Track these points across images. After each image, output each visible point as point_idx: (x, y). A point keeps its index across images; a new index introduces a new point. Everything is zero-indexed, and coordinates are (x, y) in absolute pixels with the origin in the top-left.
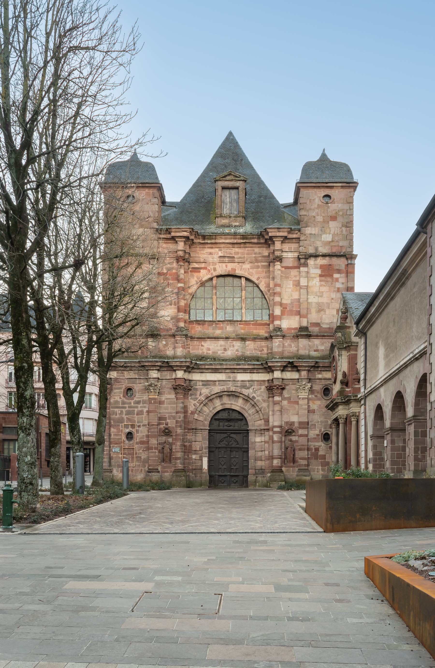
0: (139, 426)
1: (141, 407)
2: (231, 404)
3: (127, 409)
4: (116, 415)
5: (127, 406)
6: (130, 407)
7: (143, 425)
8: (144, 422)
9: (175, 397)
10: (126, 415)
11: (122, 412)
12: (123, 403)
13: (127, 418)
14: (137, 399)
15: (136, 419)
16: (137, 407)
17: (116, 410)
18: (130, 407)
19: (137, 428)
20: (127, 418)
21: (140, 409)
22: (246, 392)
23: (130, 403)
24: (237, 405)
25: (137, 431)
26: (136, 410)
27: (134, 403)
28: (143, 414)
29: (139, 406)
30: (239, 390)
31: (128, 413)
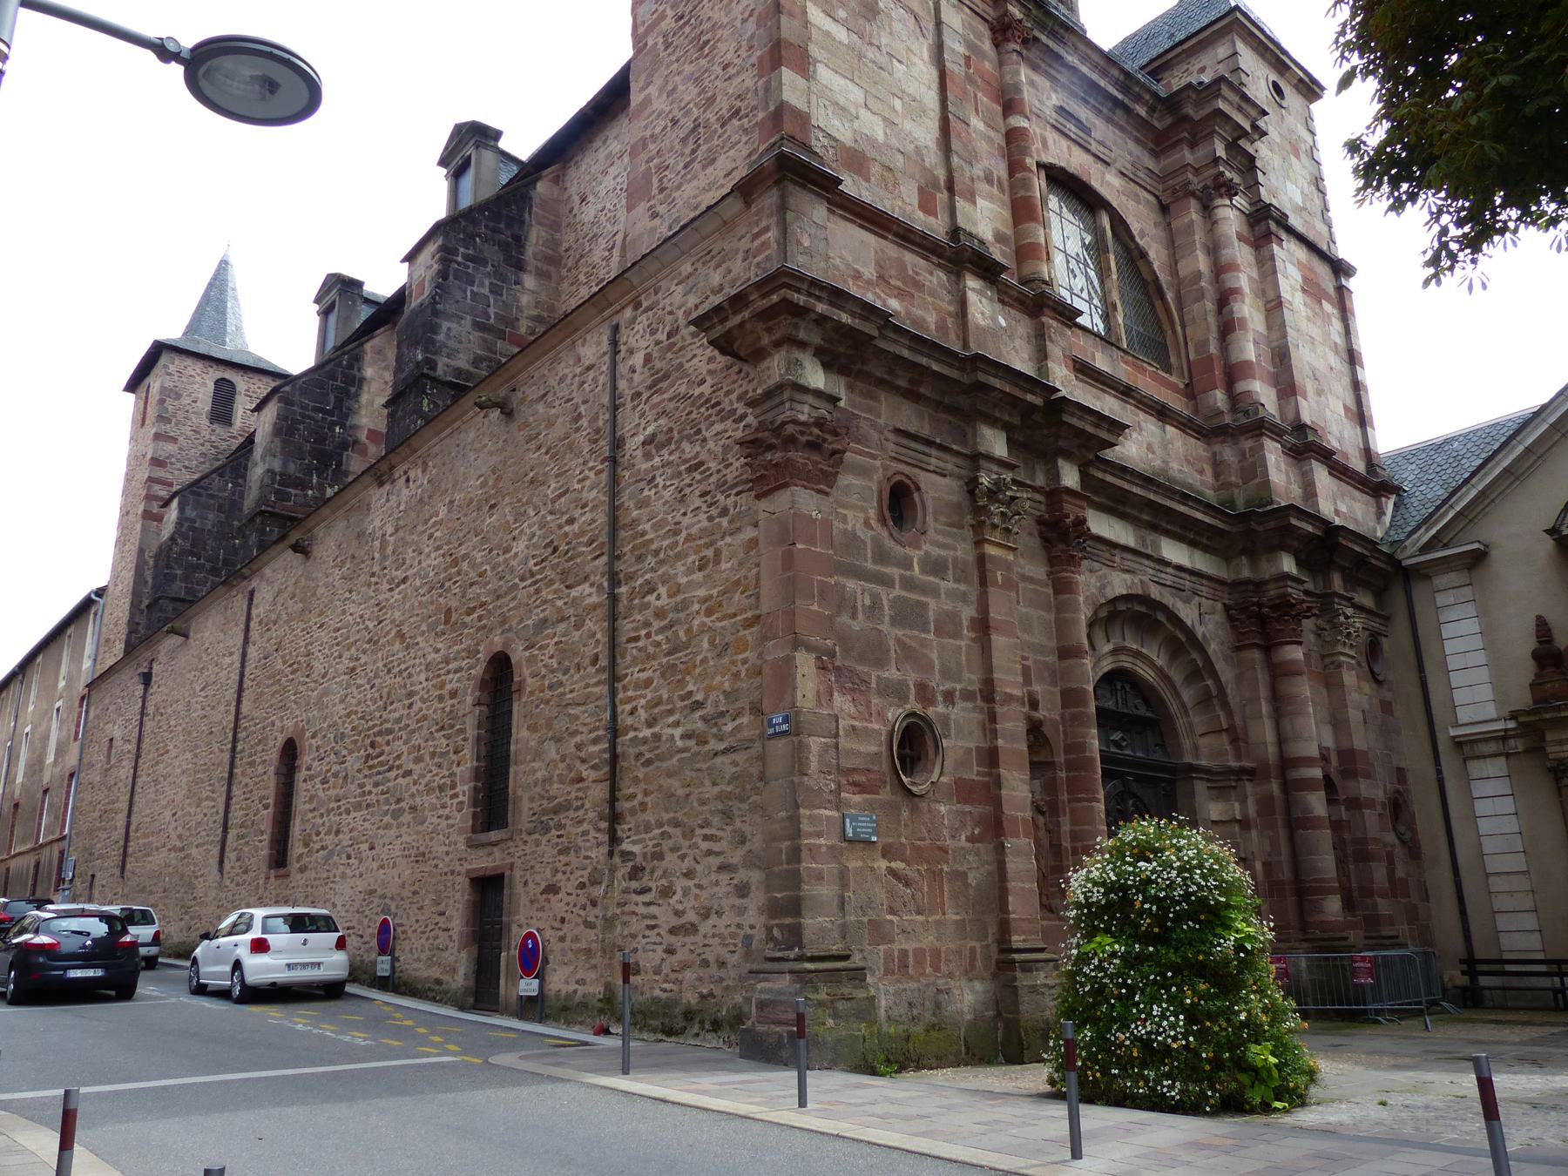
0: (949, 697)
1: (949, 593)
2: (1137, 655)
3: (897, 591)
4: (854, 616)
5: (894, 572)
6: (909, 584)
7: (967, 696)
8: (966, 675)
9: (1049, 574)
10: (895, 622)
11: (875, 607)
12: (882, 556)
13: (898, 640)
14: (936, 552)
15: (934, 656)
16: (933, 591)
17: (851, 584)
18: (909, 584)
19: (941, 709)
20: (898, 640)
21: (948, 606)
22: (1188, 613)
23: (909, 567)
24: (1150, 660)
25: (946, 720)
26: (932, 603)
27: (923, 571)
28: (957, 635)
29: (943, 584)
30: (1169, 600)
31: (908, 615)
